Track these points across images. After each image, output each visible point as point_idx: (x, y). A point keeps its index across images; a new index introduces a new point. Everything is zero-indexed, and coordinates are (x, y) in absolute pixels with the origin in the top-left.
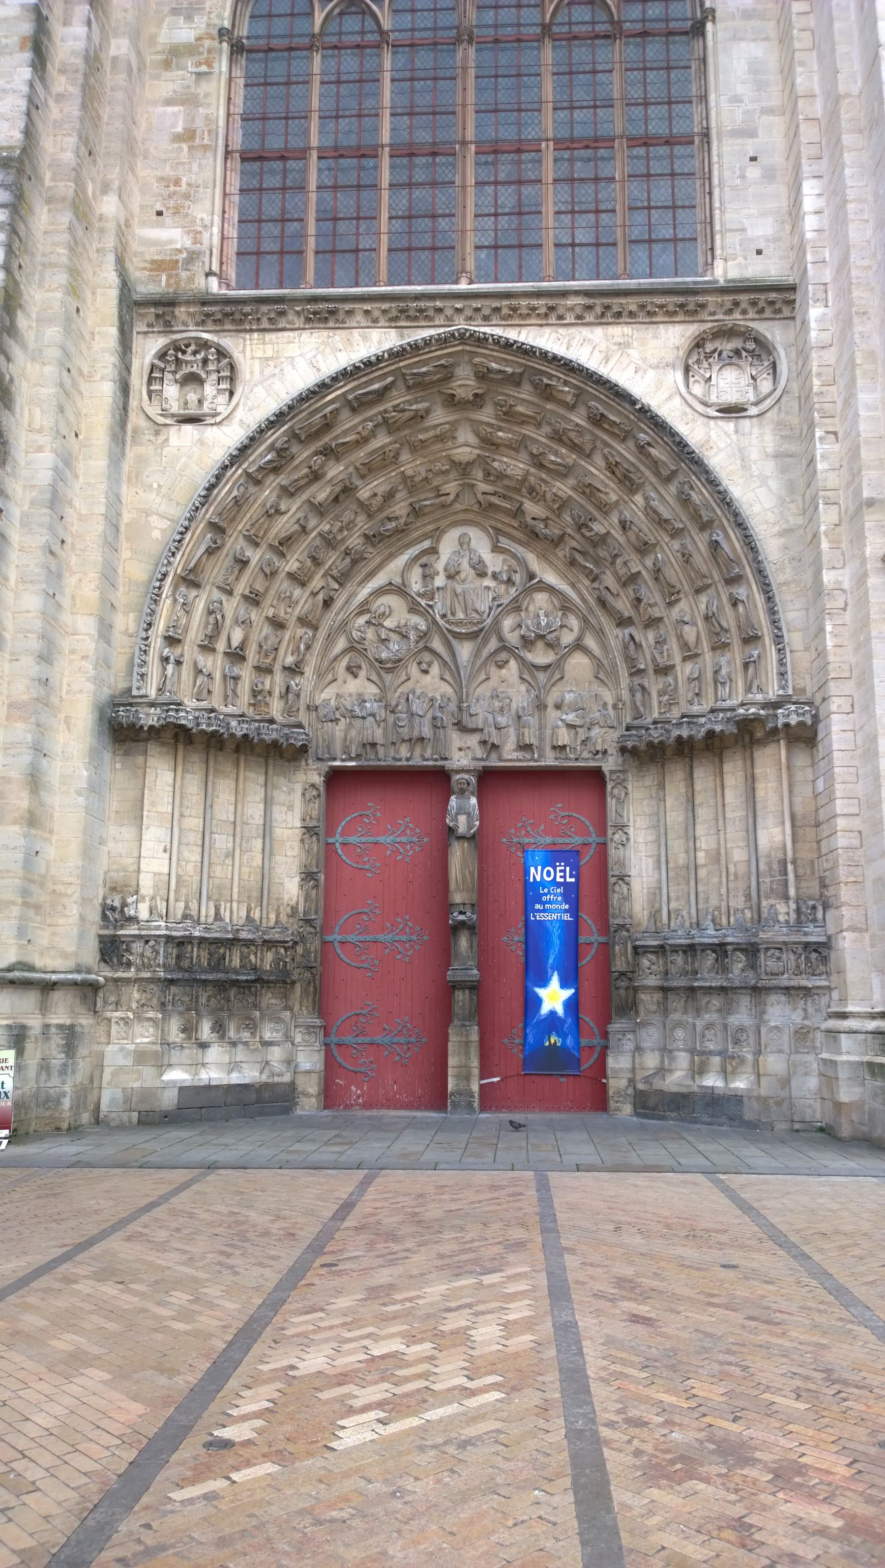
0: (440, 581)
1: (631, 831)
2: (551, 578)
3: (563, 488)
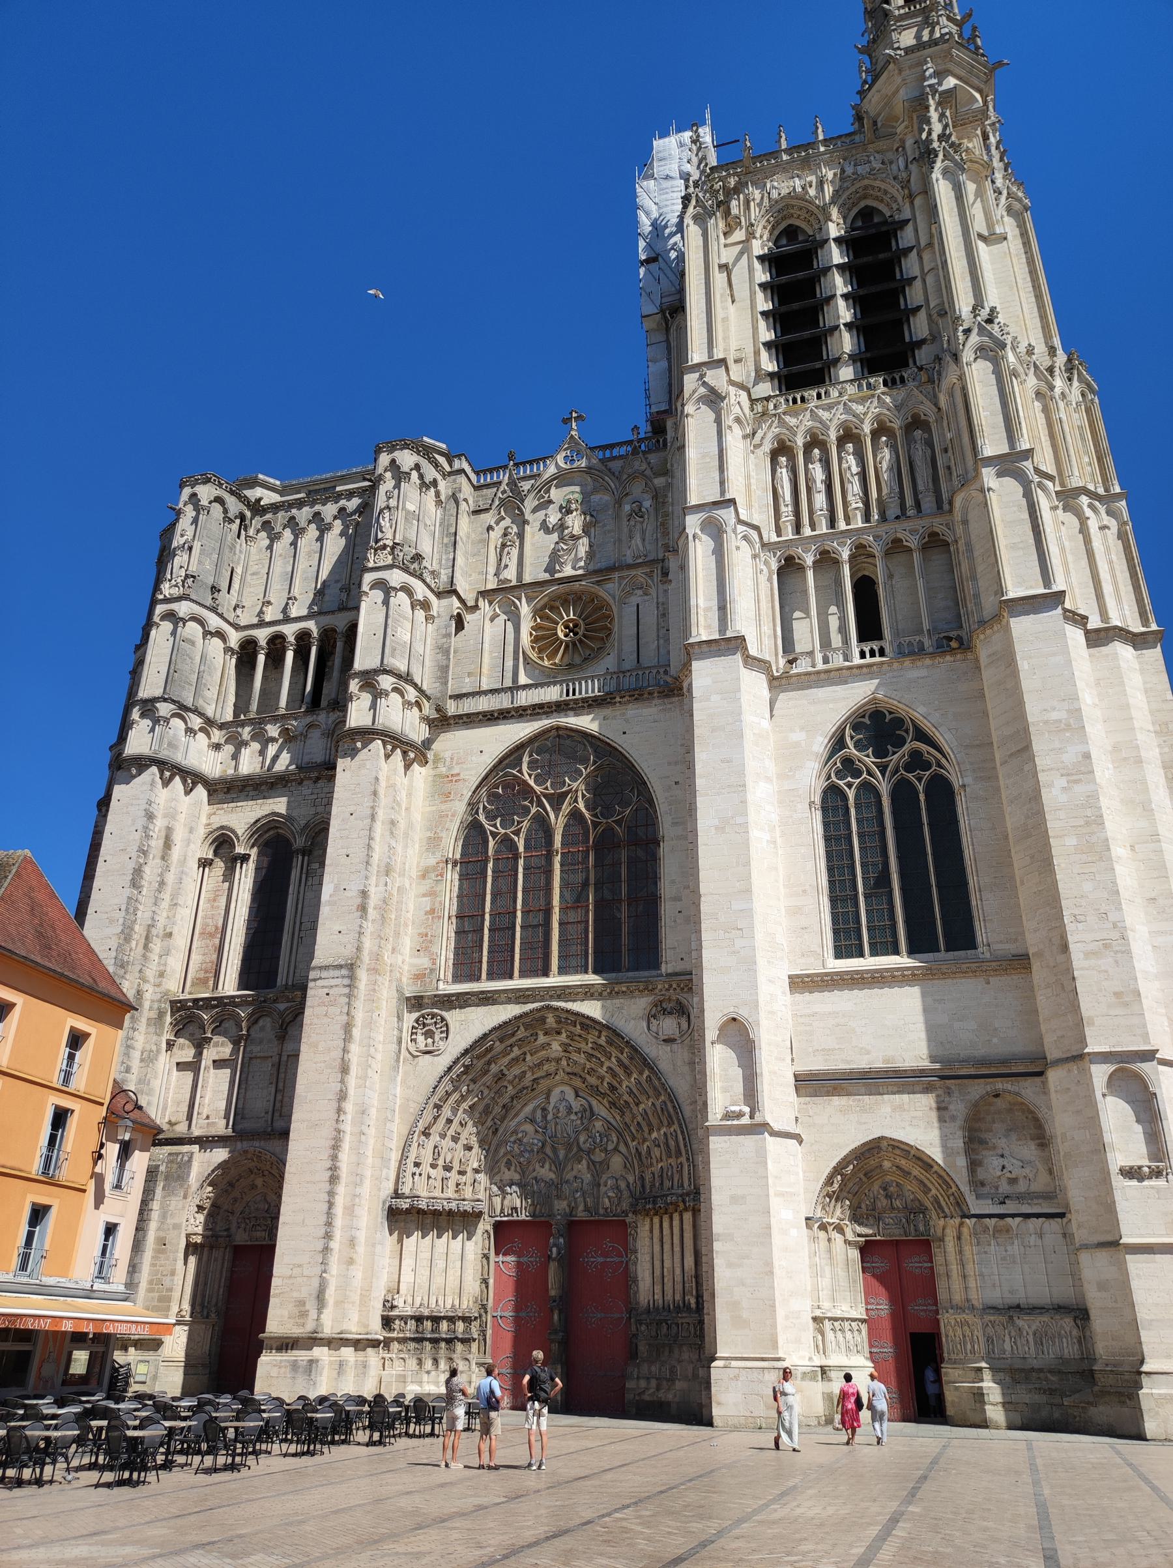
0: (550, 1117)
1: (639, 1256)
2: (603, 1112)
3: (602, 1071)
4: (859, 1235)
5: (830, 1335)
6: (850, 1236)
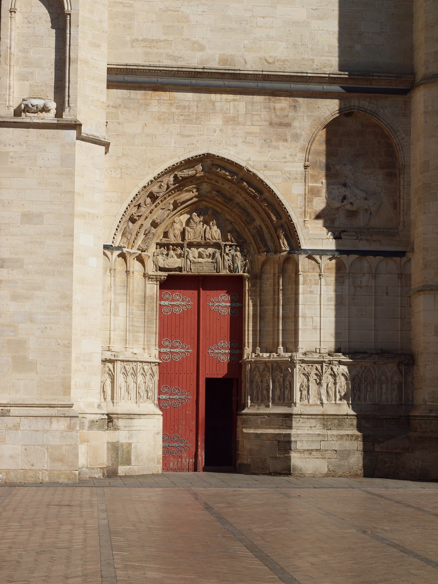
4: (161, 269)
5: (120, 379)
6: (151, 269)
